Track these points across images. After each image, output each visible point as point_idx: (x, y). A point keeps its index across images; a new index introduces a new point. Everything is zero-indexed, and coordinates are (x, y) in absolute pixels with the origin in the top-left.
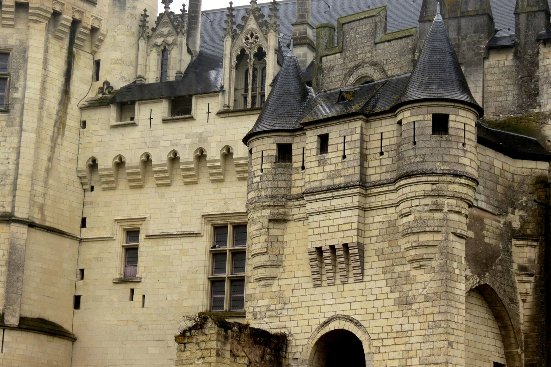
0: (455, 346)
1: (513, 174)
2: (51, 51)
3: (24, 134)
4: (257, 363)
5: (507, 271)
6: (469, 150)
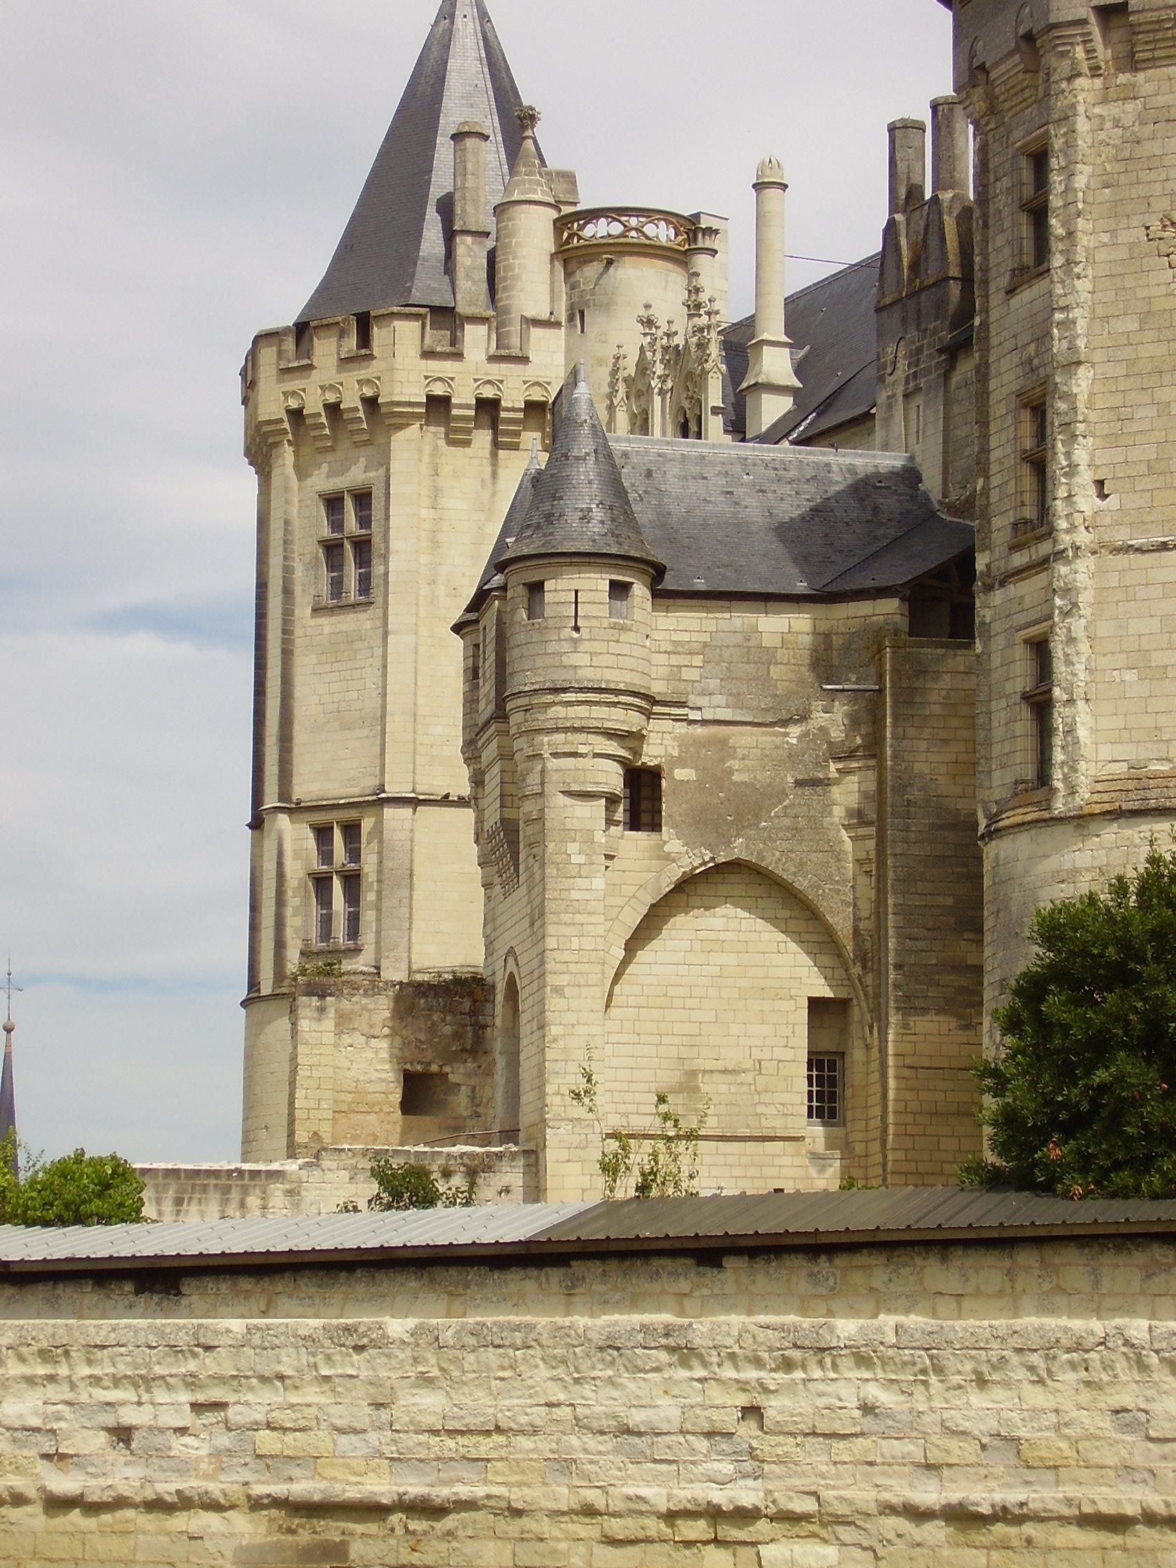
0: (567, 992)
1: (827, 635)
2: (446, 470)
3: (390, 638)
4: (422, 1042)
5: (817, 826)
6: (586, 636)
